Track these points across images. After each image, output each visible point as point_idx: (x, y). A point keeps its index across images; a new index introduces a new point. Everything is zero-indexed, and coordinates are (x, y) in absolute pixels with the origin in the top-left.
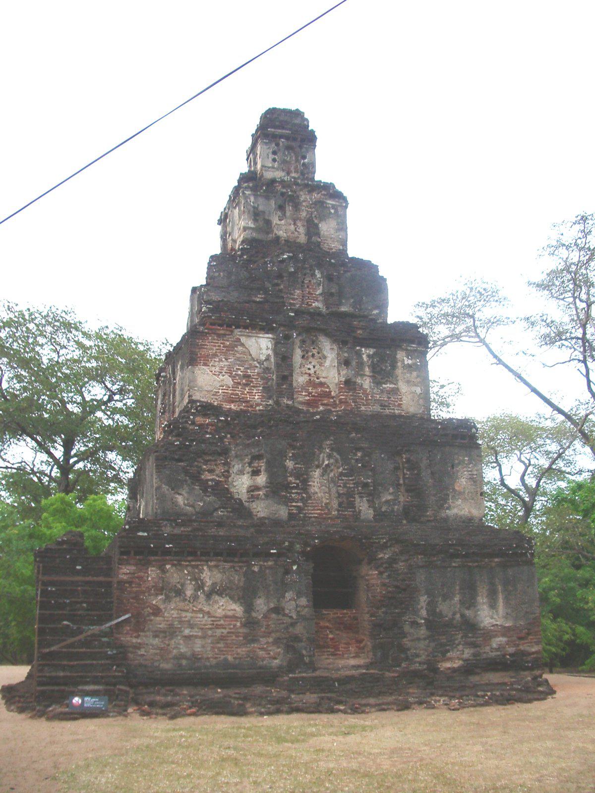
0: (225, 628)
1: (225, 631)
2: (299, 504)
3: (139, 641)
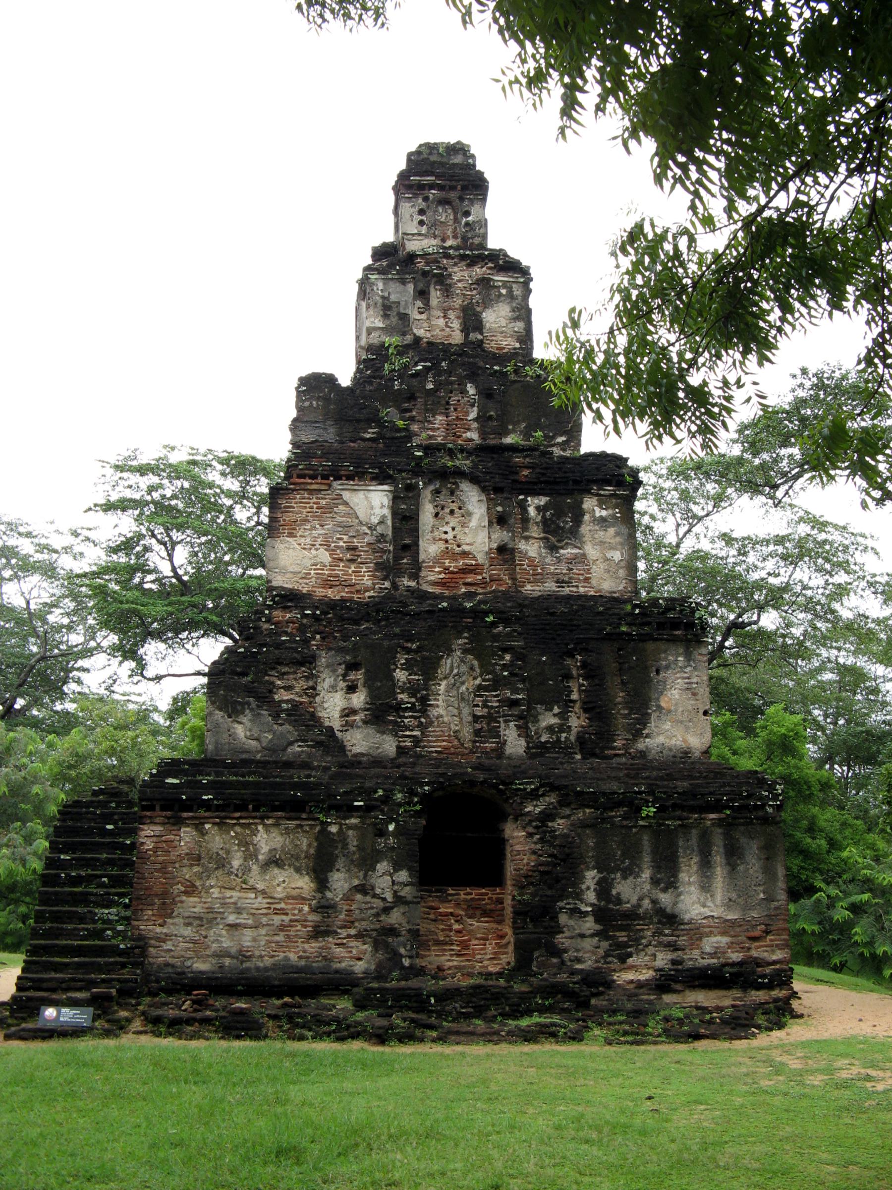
0: (287, 914)
1: (286, 919)
3: (165, 930)
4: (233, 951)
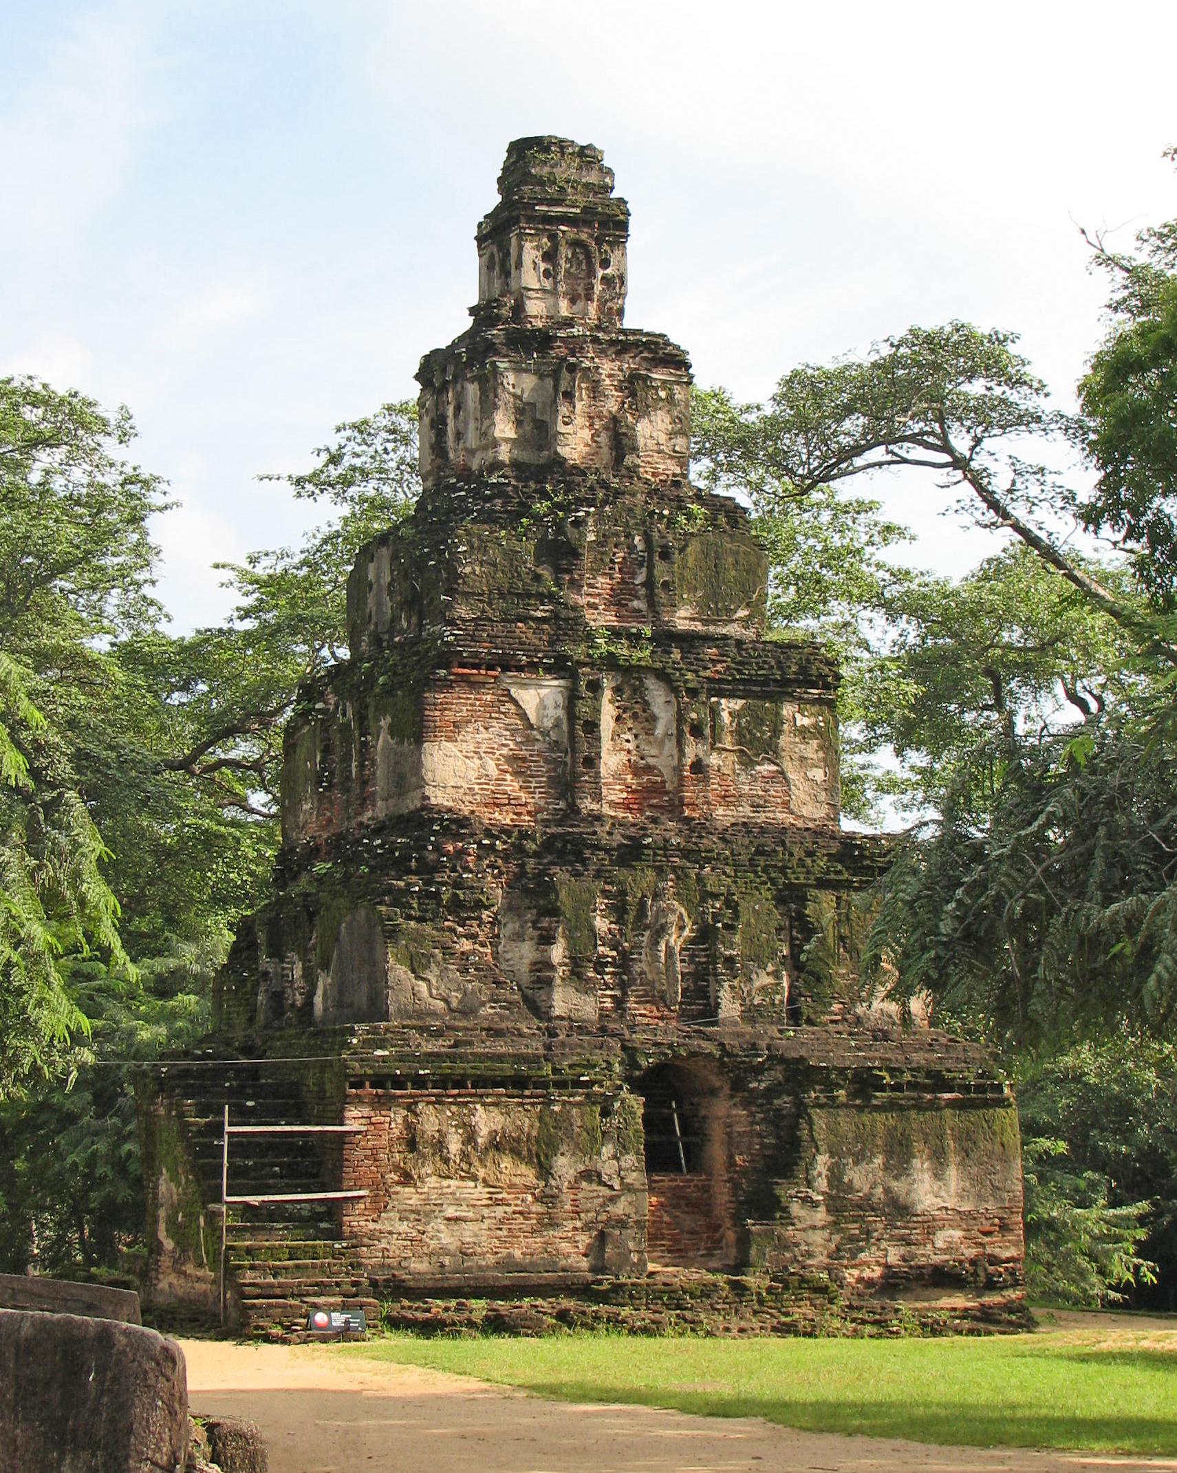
0: (509, 1205)
3: (378, 1226)
4: (452, 1248)
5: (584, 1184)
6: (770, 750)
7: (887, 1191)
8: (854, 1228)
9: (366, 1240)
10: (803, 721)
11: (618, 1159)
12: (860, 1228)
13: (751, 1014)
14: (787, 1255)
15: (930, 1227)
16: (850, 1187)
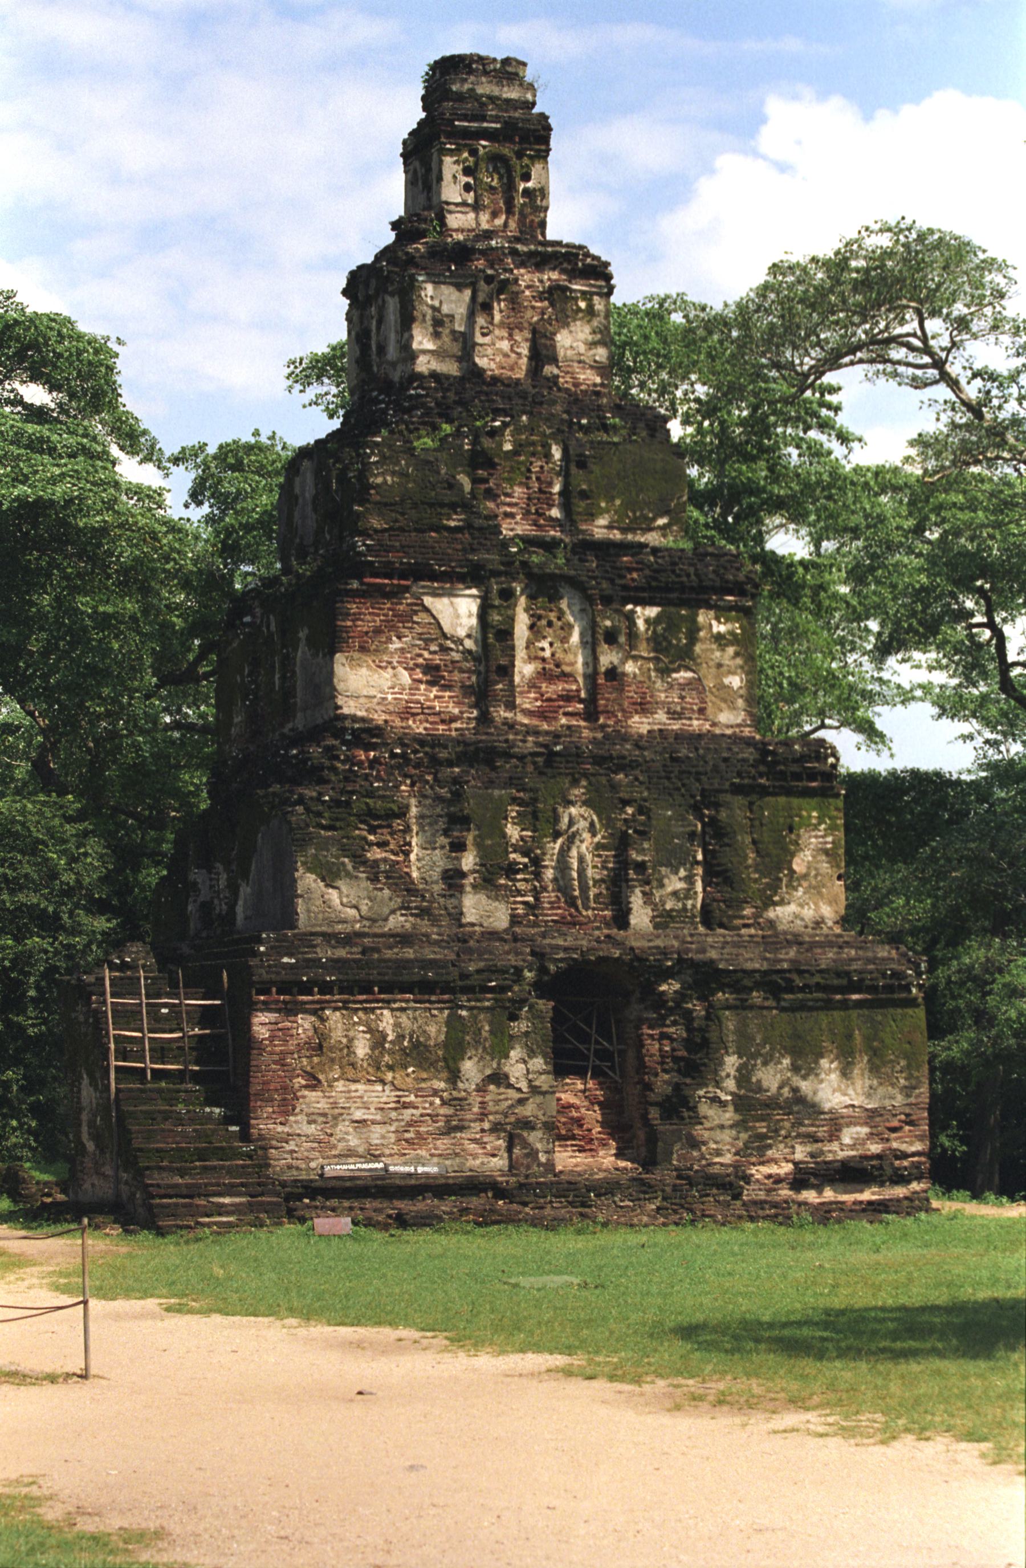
0: (417, 1108)
2: (526, 899)
3: (286, 1129)
5: (492, 1087)
6: (685, 657)
7: (795, 1090)
8: (762, 1128)
9: (274, 1143)
10: (720, 628)
11: (525, 1062)
12: (768, 1127)
13: (663, 920)
14: (695, 1154)
15: (836, 1124)
16: (759, 1088)
